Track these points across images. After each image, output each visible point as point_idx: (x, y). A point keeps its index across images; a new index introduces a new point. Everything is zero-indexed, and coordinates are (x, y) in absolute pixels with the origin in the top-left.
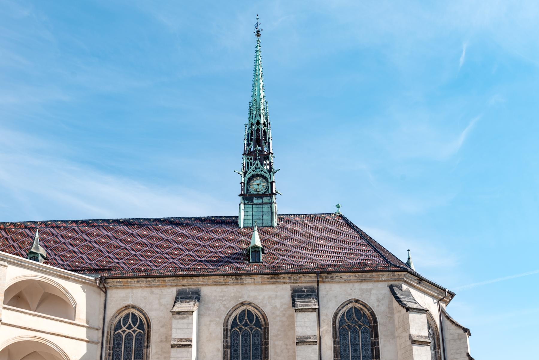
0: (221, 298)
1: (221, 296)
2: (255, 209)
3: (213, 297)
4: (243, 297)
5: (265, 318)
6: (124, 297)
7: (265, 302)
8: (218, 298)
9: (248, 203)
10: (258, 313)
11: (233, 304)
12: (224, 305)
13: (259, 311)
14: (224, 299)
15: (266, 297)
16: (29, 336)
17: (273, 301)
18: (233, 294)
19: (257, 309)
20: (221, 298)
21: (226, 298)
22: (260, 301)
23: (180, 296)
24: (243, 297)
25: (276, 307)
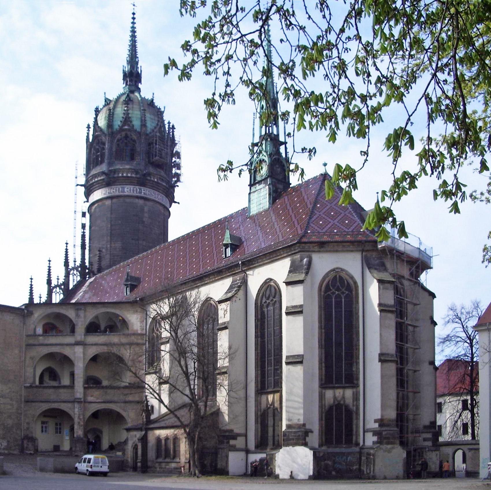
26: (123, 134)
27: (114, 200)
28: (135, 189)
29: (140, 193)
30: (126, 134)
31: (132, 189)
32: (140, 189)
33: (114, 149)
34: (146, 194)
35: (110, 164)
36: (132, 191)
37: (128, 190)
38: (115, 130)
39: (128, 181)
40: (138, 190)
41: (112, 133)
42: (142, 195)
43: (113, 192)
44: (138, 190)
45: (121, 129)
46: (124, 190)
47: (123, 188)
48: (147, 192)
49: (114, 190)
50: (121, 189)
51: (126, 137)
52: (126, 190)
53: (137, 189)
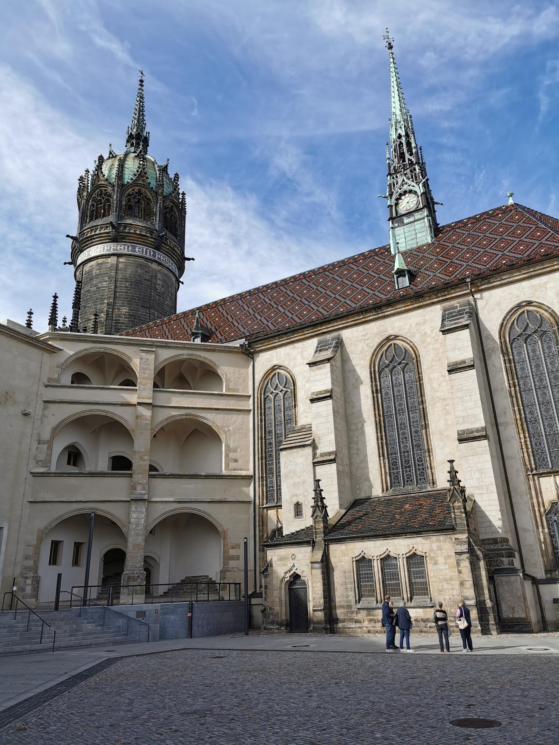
0: (363, 338)
1: (363, 336)
2: (406, 230)
3: (355, 339)
4: (388, 331)
5: (415, 349)
6: (269, 358)
7: (412, 331)
8: (360, 338)
9: (399, 225)
10: (406, 345)
11: (378, 340)
12: (368, 344)
13: (407, 343)
14: (366, 338)
15: (414, 325)
16: (181, 415)
17: (422, 328)
18: (376, 330)
19: (405, 341)
20: (363, 338)
21: (369, 336)
22: (406, 331)
23: (320, 345)
24: (388, 331)
25: (426, 333)
26: (137, 189)
27: (121, 260)
28: (148, 251)
29: (155, 256)
30: (139, 190)
31: (145, 249)
32: (154, 252)
33: (124, 203)
34: (160, 260)
35: (120, 217)
36: (144, 253)
37: (141, 250)
38: (126, 182)
39: (141, 239)
40: (152, 253)
41: (123, 185)
42: (156, 259)
43: (121, 249)
44: (152, 253)
45: (135, 183)
46: (135, 249)
47: (134, 247)
48: (162, 258)
49: (122, 248)
50: (130, 248)
51: (139, 193)
52: (137, 249)
53: (150, 252)
